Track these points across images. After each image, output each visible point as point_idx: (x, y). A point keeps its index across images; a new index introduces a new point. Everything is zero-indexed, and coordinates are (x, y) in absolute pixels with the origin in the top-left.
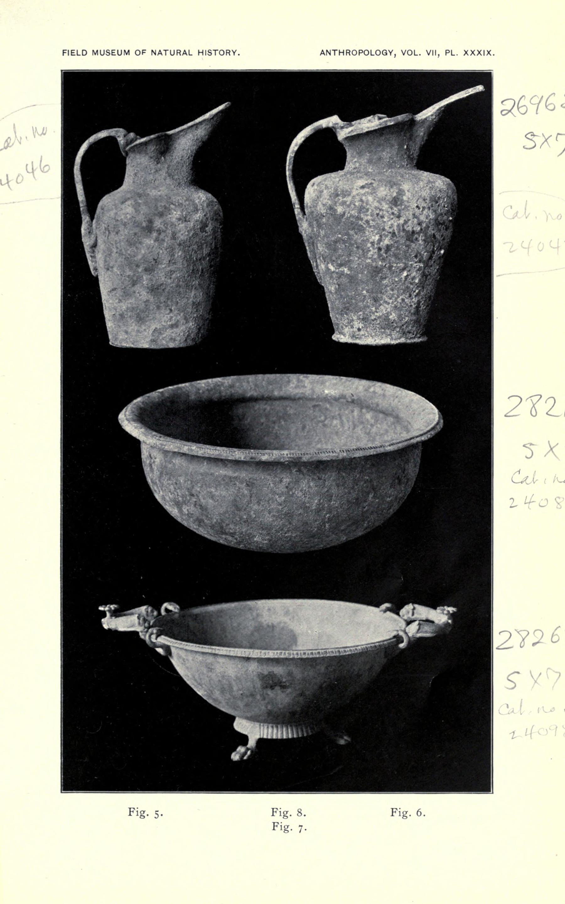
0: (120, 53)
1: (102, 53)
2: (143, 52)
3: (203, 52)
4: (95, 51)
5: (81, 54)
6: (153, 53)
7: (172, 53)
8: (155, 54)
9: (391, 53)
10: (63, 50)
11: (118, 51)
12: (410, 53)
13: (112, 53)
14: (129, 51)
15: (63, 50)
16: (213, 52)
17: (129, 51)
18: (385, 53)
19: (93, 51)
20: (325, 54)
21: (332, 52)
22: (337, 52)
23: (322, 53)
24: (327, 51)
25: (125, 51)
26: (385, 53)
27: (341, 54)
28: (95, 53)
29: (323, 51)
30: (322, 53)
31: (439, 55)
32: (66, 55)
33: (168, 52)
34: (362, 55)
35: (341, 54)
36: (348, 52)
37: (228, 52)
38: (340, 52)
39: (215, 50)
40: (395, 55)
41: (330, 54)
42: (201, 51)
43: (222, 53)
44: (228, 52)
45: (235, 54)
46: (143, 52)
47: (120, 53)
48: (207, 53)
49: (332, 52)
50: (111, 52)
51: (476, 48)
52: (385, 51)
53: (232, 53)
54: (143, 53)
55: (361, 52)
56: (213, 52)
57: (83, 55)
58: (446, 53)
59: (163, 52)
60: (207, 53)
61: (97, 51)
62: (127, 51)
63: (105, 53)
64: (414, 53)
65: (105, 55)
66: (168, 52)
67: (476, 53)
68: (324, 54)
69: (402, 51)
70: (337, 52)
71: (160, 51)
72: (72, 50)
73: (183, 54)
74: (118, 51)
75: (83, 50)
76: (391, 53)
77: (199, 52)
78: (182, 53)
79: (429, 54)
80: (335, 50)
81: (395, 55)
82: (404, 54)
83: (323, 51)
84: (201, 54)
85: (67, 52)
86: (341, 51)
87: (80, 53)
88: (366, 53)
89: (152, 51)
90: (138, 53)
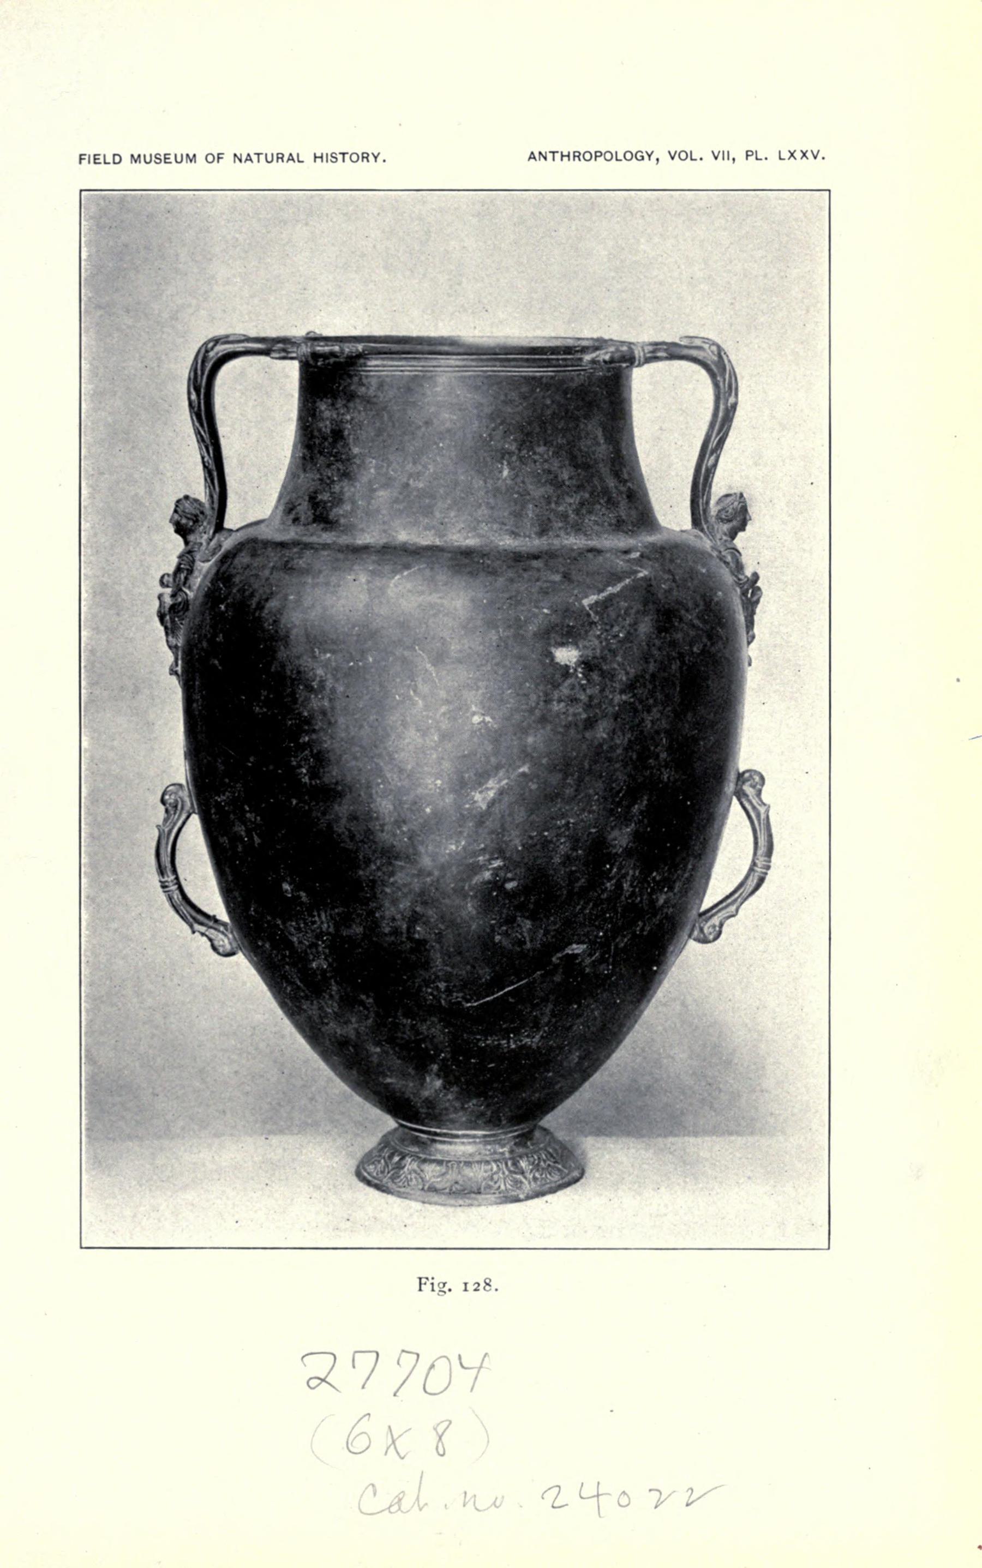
0: (179, 160)
1: (148, 160)
2: (219, 157)
3: (322, 157)
4: (136, 157)
5: (111, 161)
6: (237, 160)
7: (269, 159)
8: (240, 161)
9: (649, 156)
10: (81, 155)
11: (176, 156)
12: (683, 156)
14: (194, 155)
15: (81, 155)
16: (340, 157)
17: (194, 155)
18: (638, 156)
19: (132, 156)
20: (537, 157)
21: (550, 156)
22: (558, 156)
23: (532, 156)
24: (540, 153)
25: (188, 155)
26: (638, 156)
27: (565, 159)
28: (135, 159)
29: (532, 153)
30: (532, 156)
31: (734, 159)
32: (85, 162)
33: (262, 157)
34: (601, 159)
35: (565, 159)
36: (577, 156)
37: (365, 157)
38: (562, 156)
39: (344, 154)
40: (658, 160)
41: (545, 158)
42: (318, 155)
43: (354, 158)
44: (365, 157)
45: (380, 159)
46: (219, 157)
47: (179, 160)
48: (329, 157)
49: (550, 156)
50: (162, 158)
51: (798, 147)
52: (639, 154)
53: (371, 158)
54: (219, 158)
55: (597, 155)
57: (114, 163)
58: (747, 155)
59: (254, 158)
60: (329, 157)
61: (139, 156)
62: (191, 156)
63: (153, 158)
64: (690, 156)
66: (262, 157)
67: (798, 155)
68: (534, 158)
69: (669, 153)
70: (558, 156)
71: (249, 155)
73: (289, 159)
74: (176, 156)
75: (114, 155)
76: (649, 156)
77: (316, 157)
78: (285, 159)
79: (716, 158)
80: (553, 153)
81: (658, 160)
82: (673, 158)
83: (532, 153)
84: (318, 160)
85: (87, 157)
86: (565, 153)
87: (109, 159)
88: (608, 156)
89: (235, 155)
90: (210, 158)
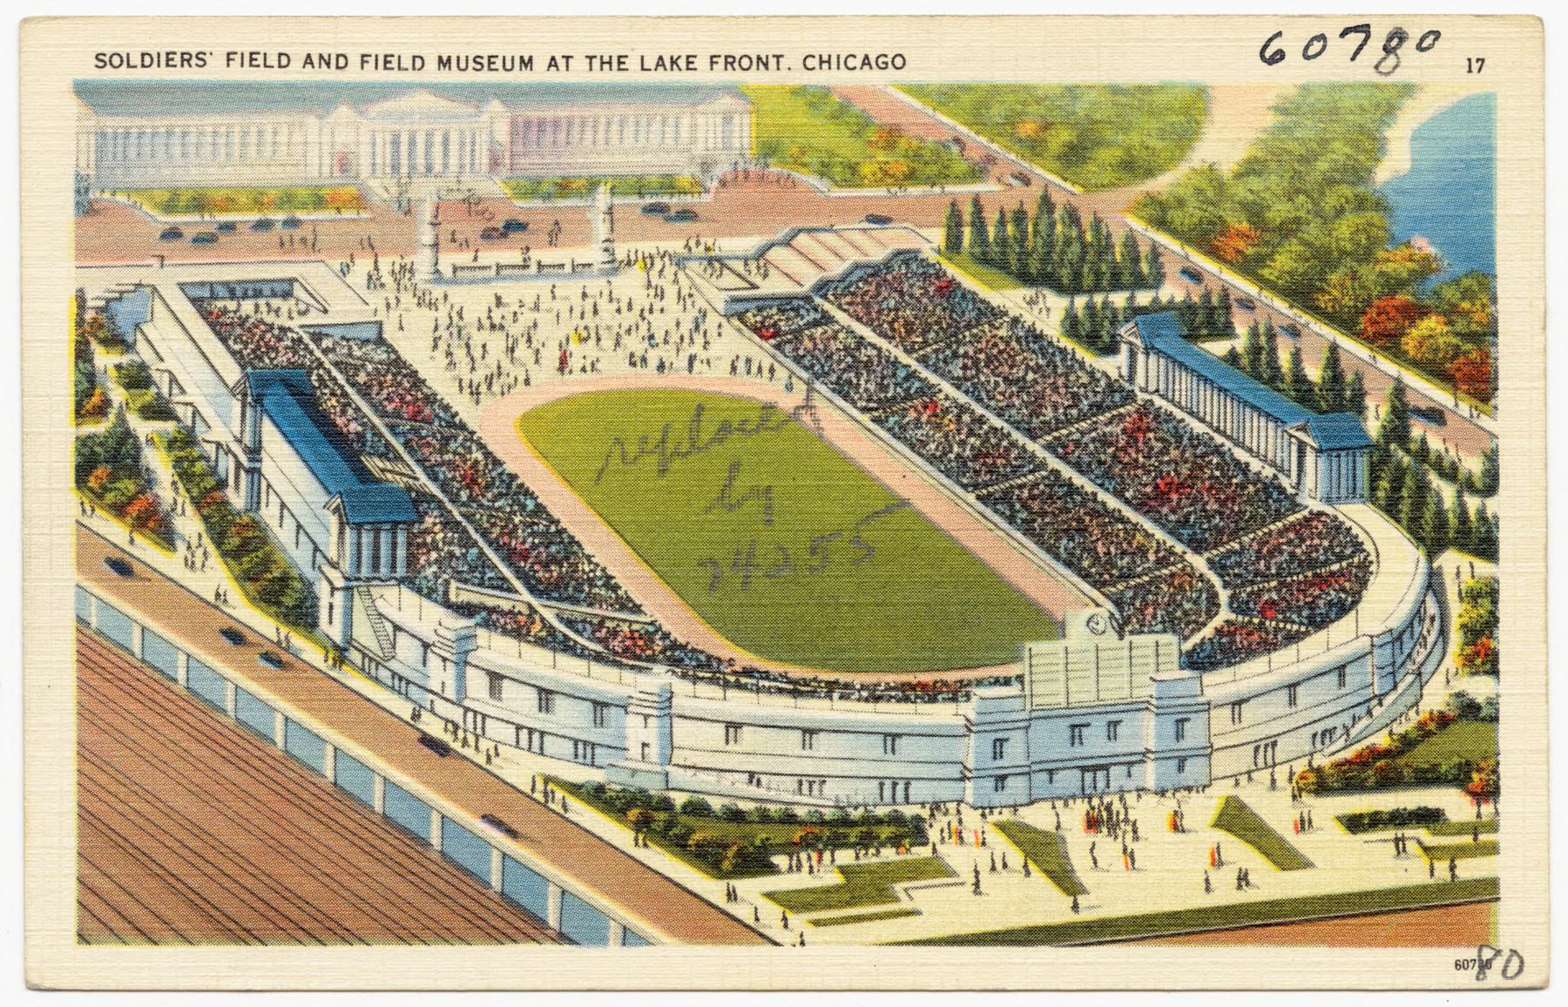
0: (509, 66)
1: (463, 65)
4: (445, 59)
5: (410, 67)
13: (490, 63)
17: (530, 59)
19: (440, 58)
25: (522, 57)
28: (444, 63)
47: (509, 66)
50: (485, 62)
56: (772, 62)
61: (449, 59)
62: (526, 59)
65: (470, 68)
72: (386, 56)
75: (414, 57)
85: (372, 60)
87: (407, 63)
